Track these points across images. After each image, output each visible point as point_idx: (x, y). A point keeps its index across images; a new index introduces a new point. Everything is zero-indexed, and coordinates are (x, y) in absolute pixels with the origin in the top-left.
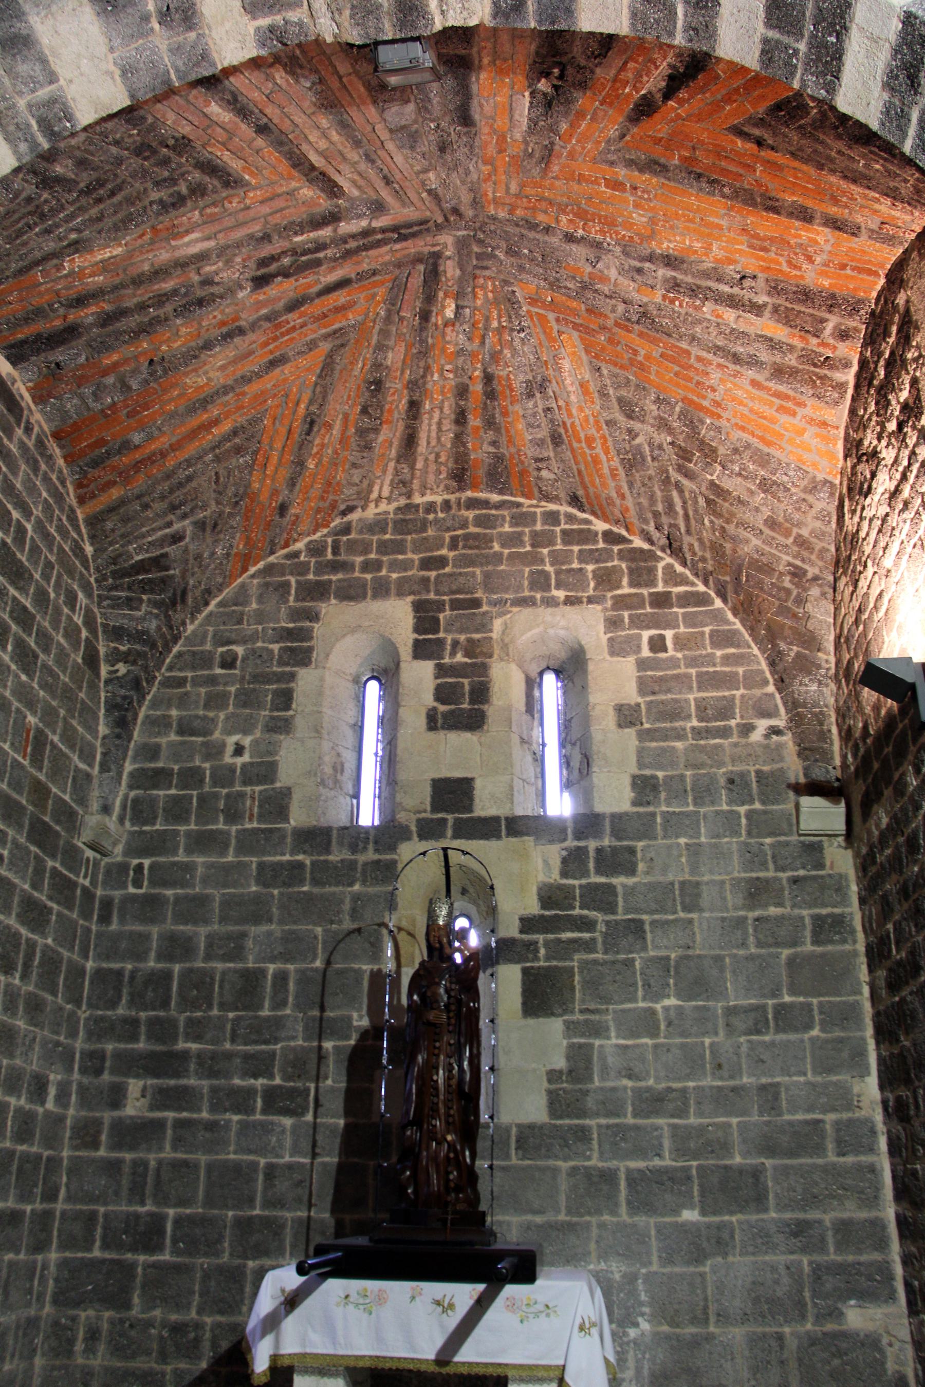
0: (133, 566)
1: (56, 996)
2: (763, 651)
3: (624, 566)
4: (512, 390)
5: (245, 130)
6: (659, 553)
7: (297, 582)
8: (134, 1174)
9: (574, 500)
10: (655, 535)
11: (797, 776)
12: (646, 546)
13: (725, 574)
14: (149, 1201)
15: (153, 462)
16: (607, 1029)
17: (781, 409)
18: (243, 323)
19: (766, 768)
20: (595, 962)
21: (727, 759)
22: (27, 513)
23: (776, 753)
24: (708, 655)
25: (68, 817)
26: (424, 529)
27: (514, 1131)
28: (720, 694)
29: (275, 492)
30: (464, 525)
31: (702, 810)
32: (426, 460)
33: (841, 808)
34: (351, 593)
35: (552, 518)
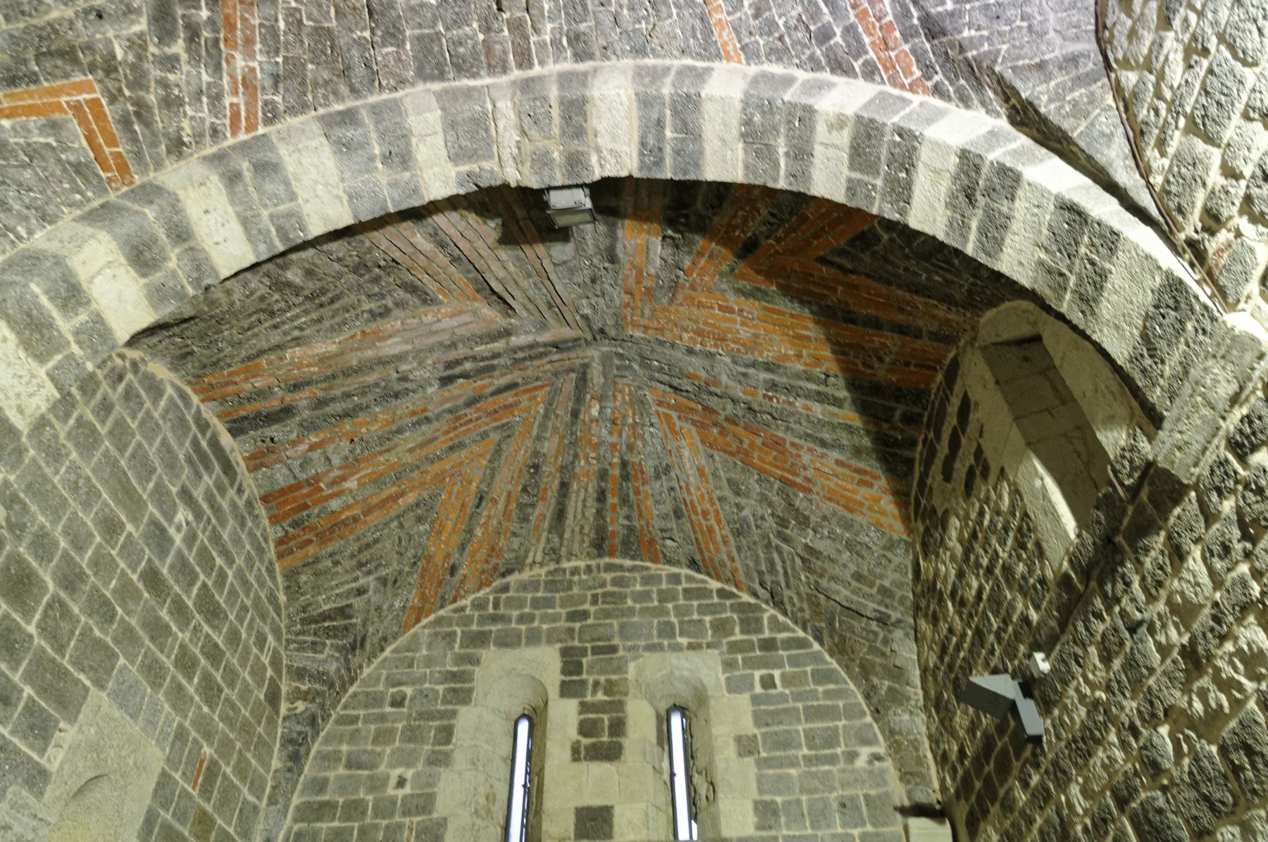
2: (858, 686)
3: (735, 617)
4: (642, 473)
5: (442, 259)
6: (764, 606)
7: (463, 632)
9: (693, 564)
10: (761, 591)
11: (901, 799)
12: (753, 601)
13: (821, 621)
15: (346, 525)
17: (862, 483)
18: (429, 414)
19: (873, 792)
21: (837, 784)
22: (230, 561)
23: (879, 779)
24: (811, 691)
26: (570, 587)
28: (825, 725)
29: (448, 556)
30: (603, 585)
31: (820, 833)
32: (573, 531)
33: (947, 829)
34: (507, 642)
35: (675, 579)
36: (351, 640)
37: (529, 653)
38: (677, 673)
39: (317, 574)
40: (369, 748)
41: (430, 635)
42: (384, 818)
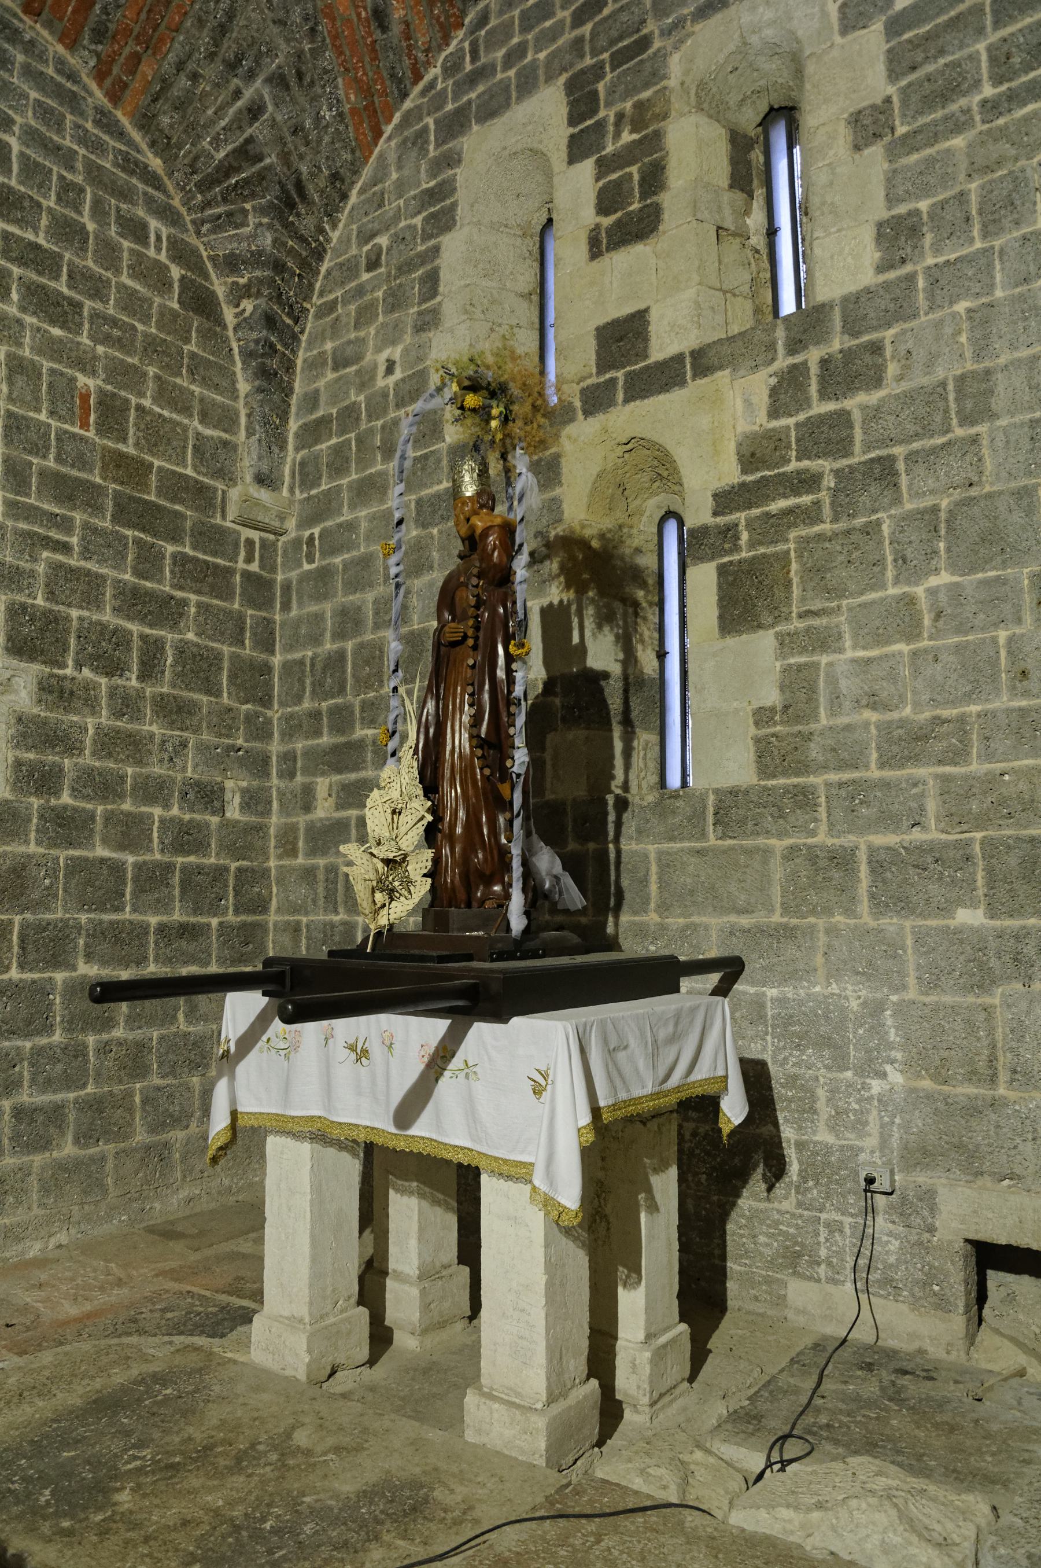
0: (218, 169)
1: (218, 694)
8: (327, 880)
14: (341, 910)
16: (840, 636)
20: (820, 537)
25: (202, 496)
27: (712, 797)
31: (997, 243)
36: (276, 190)
37: (521, 112)
38: (754, 39)
39: (180, 106)
40: (353, 336)
41: (398, 147)
42: (377, 419)
